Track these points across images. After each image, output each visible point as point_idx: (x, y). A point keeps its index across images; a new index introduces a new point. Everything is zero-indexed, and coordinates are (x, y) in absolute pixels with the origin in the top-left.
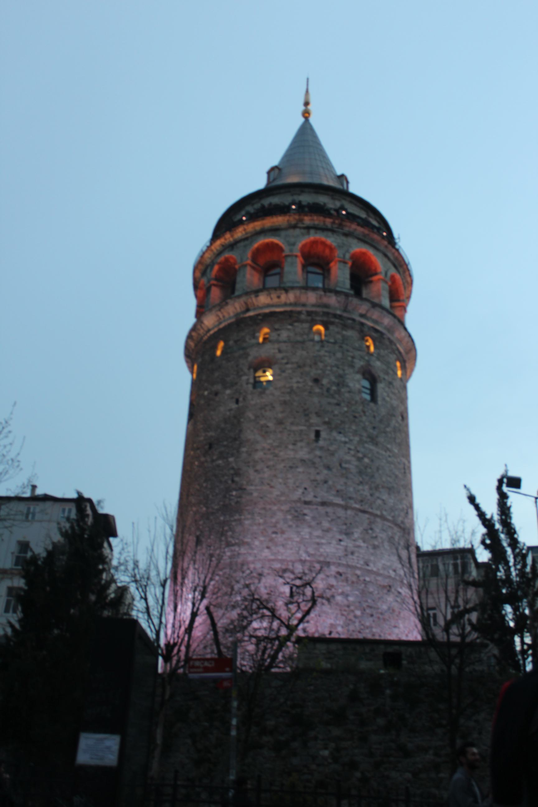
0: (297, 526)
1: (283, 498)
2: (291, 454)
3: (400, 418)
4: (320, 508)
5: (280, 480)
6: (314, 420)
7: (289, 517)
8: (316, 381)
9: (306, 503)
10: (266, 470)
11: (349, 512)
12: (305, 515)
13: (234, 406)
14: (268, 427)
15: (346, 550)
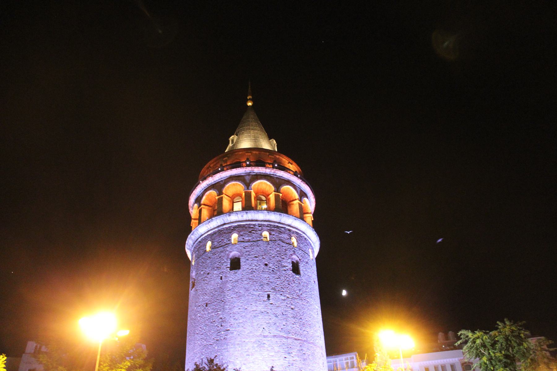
0: (260, 350)
1: (251, 335)
2: (255, 308)
3: (313, 282)
4: (272, 339)
5: (249, 324)
6: (267, 288)
7: (256, 345)
8: (266, 265)
9: (265, 337)
10: (241, 318)
11: (290, 341)
12: (264, 343)
13: (220, 281)
14: (240, 293)
15: (289, 363)
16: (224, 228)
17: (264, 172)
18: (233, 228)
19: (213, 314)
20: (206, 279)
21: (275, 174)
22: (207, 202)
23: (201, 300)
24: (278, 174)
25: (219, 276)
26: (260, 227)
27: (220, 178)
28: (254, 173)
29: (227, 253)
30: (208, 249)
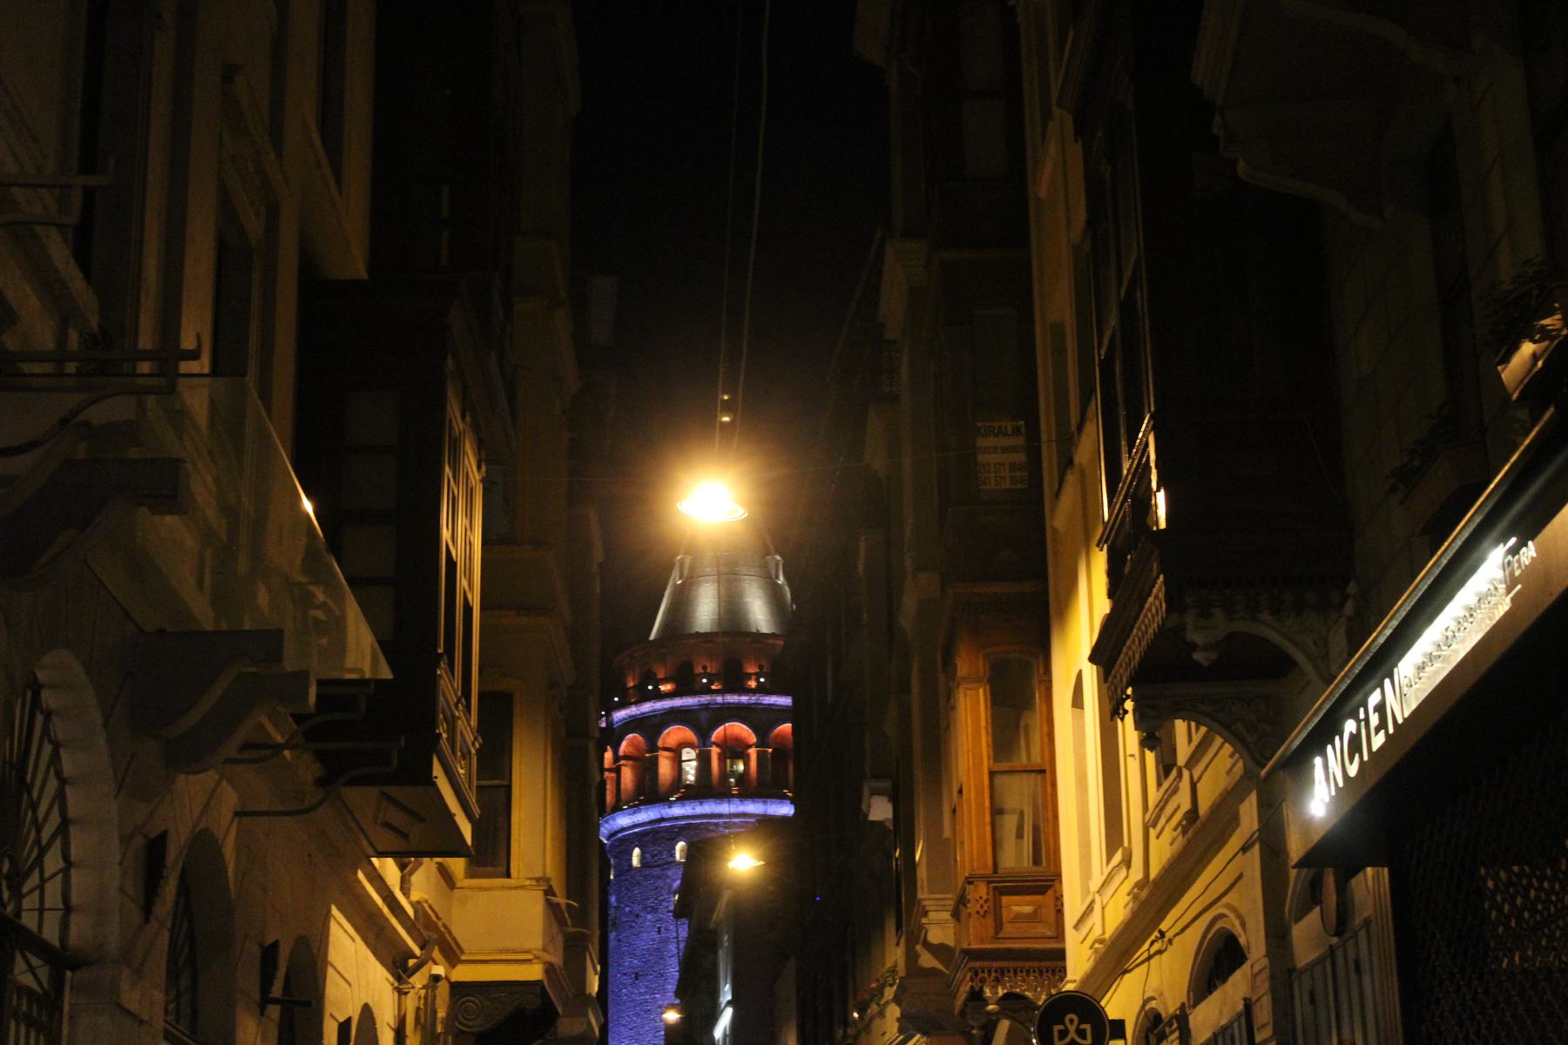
13: (657, 937)
16: (661, 827)
17: (736, 701)
18: (676, 830)
19: (647, 997)
20: (633, 924)
21: (759, 702)
22: (631, 750)
23: (627, 964)
24: (764, 702)
25: (654, 926)
26: (726, 828)
27: (651, 709)
28: (717, 704)
29: (668, 881)
30: (636, 861)
